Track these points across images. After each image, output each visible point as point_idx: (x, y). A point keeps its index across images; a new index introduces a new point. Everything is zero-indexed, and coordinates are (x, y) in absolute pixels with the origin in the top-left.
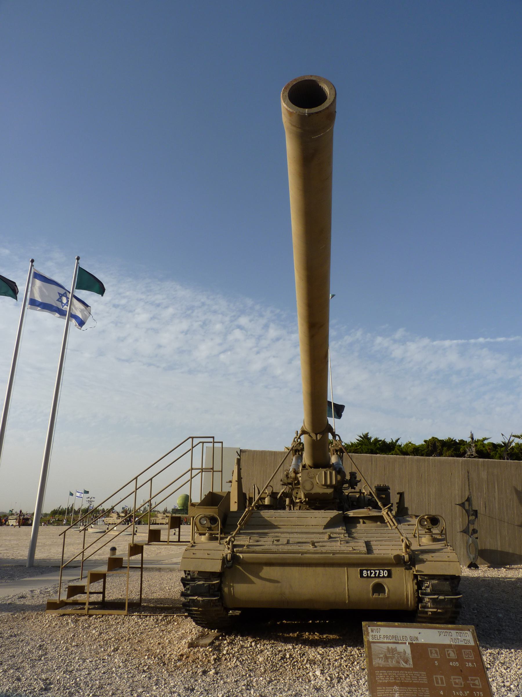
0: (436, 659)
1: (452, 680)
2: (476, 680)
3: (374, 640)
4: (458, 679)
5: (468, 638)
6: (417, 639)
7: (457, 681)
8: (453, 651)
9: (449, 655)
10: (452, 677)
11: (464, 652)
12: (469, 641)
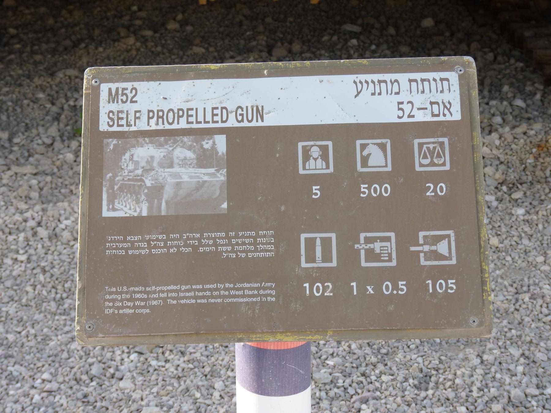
1: (361, 247)
2: (442, 238)
3: (115, 129)
5: (446, 97)
6: (260, 113)
7: (377, 246)
8: (383, 147)
9: (365, 160)
10: (362, 236)
12: (448, 106)
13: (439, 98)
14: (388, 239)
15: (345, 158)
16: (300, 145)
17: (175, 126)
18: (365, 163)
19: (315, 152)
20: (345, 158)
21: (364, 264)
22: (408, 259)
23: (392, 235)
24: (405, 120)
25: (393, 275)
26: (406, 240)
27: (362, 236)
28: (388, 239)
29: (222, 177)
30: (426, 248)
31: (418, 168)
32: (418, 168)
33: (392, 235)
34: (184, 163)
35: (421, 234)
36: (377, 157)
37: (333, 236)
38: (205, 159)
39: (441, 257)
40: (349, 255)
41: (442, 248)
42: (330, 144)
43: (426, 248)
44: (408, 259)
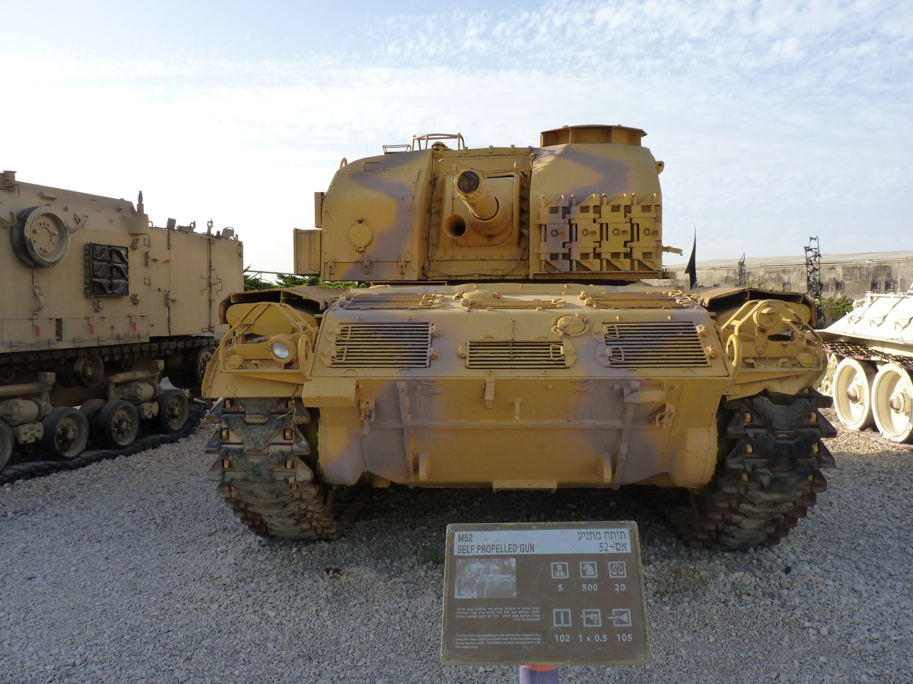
0: (559, 581)
1: (584, 616)
3: (462, 554)
4: (594, 613)
5: (623, 541)
6: (532, 547)
7: (591, 616)
8: (593, 565)
9: (584, 572)
10: (584, 611)
11: (612, 565)
12: (624, 546)
13: (620, 541)
14: (597, 613)
15: (574, 571)
16: (552, 564)
17: (490, 554)
18: (584, 574)
19: (560, 568)
20: (574, 571)
21: (585, 625)
22: (607, 623)
23: (599, 610)
24: (604, 552)
25: (600, 631)
26: (606, 613)
27: (584, 611)
28: (597, 613)
29: (514, 579)
30: (616, 618)
31: (611, 577)
32: (611, 577)
33: (599, 610)
34: (495, 572)
35: (614, 610)
36: (590, 571)
37: (569, 610)
38: (505, 570)
39: (625, 623)
40: (577, 621)
41: (624, 617)
42: (567, 564)
43: (616, 618)
44: (607, 623)
